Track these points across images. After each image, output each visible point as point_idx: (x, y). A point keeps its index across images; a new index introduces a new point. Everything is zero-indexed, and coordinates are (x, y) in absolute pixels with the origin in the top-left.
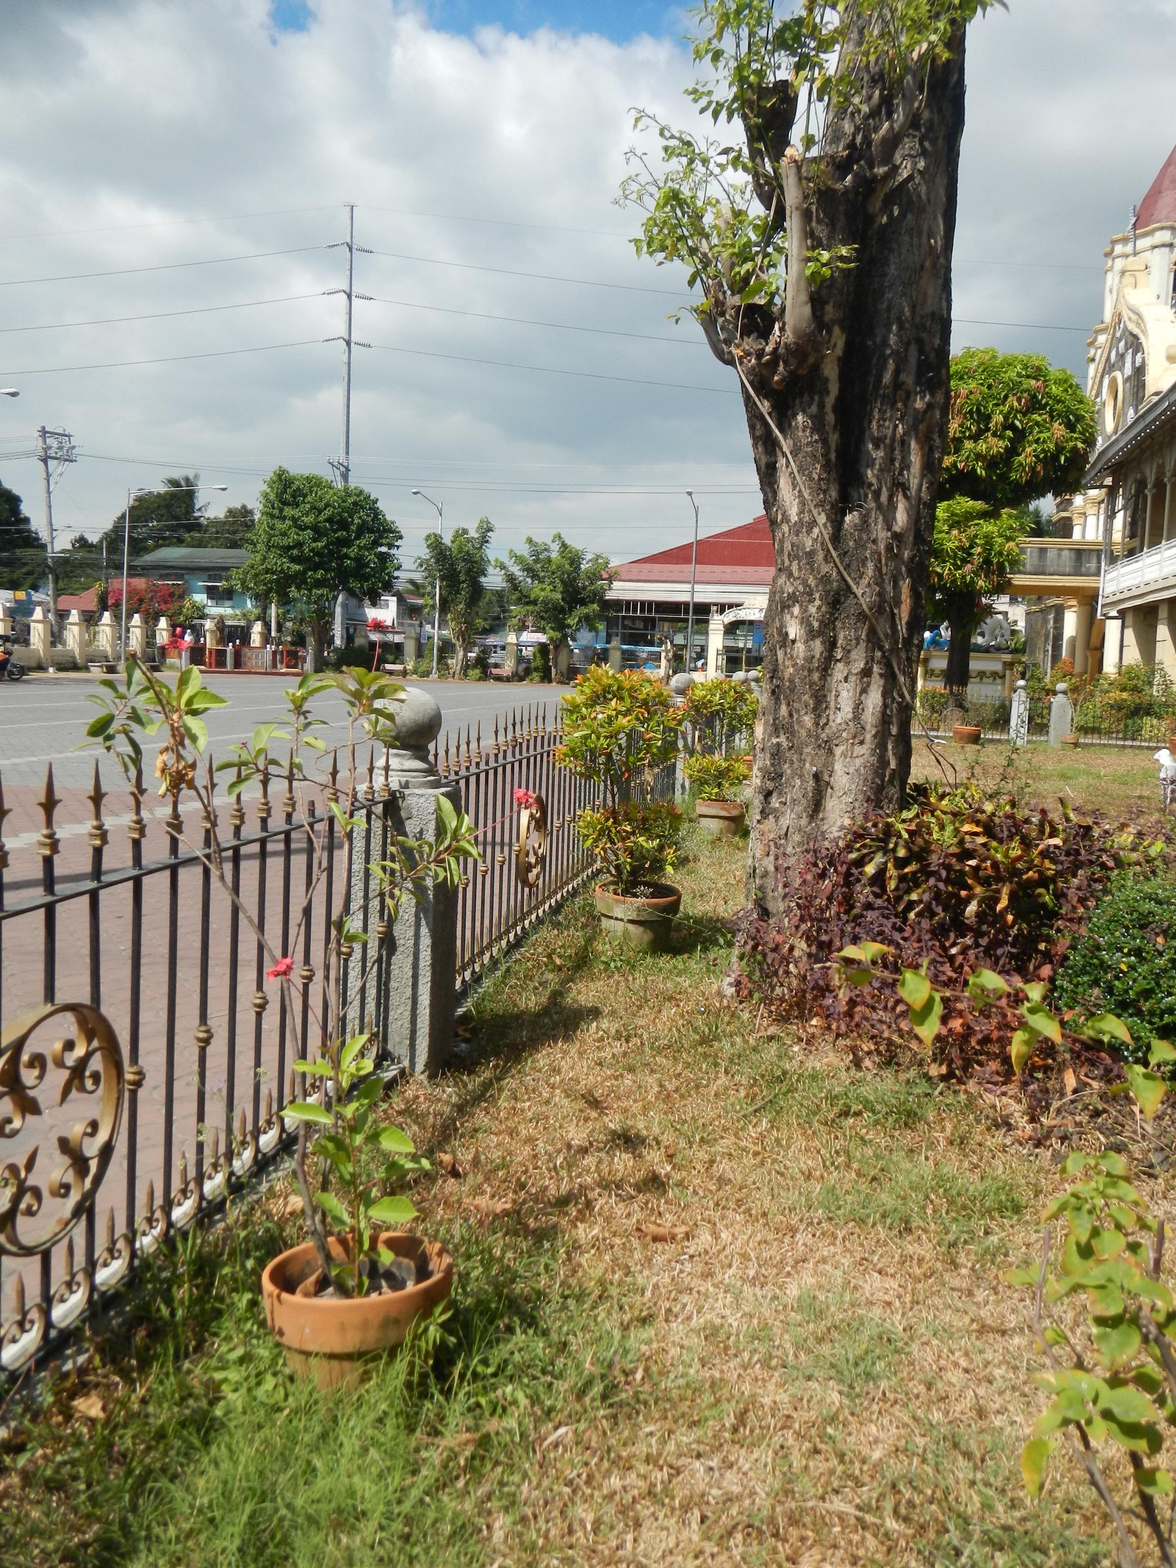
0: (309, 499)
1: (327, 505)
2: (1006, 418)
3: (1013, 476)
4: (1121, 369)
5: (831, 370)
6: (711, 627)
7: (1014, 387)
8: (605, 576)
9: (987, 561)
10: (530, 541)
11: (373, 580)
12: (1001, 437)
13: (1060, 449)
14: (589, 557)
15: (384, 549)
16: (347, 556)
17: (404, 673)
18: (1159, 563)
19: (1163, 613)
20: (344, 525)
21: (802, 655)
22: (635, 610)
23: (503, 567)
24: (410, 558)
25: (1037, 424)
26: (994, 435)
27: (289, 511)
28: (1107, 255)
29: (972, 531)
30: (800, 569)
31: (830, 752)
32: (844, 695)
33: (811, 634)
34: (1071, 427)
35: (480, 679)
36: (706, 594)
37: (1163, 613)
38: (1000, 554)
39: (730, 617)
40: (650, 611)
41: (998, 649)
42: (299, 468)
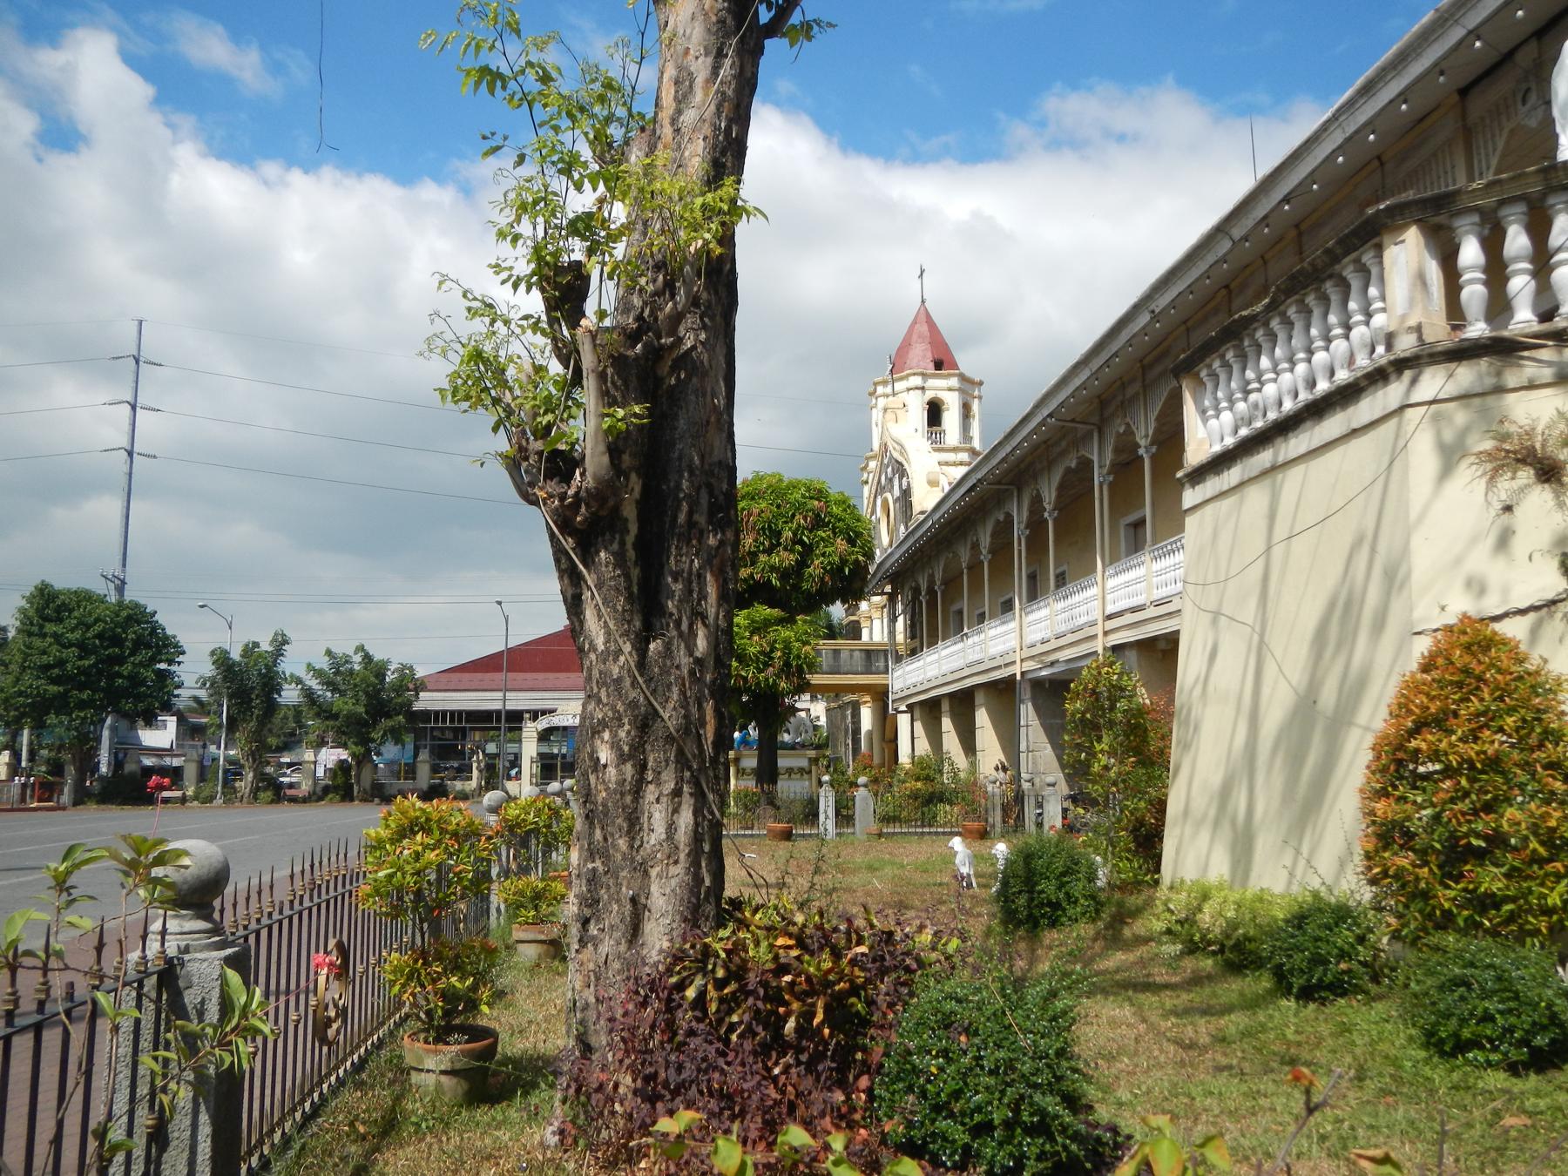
0: (76, 614)
1: (97, 620)
2: (795, 534)
3: (805, 586)
4: (891, 491)
5: (630, 512)
7: (799, 507)
8: (411, 686)
9: (787, 664)
10: (329, 653)
11: (151, 699)
12: (792, 551)
13: (844, 562)
15: (163, 666)
16: (119, 675)
17: (183, 800)
18: (937, 661)
19: (945, 706)
20: (117, 641)
21: (613, 779)
22: (444, 721)
23: (299, 681)
24: (193, 673)
25: (822, 539)
26: (785, 549)
27: (50, 628)
28: (871, 394)
29: (771, 636)
30: (608, 696)
31: (646, 874)
32: (657, 817)
33: (622, 758)
34: (851, 542)
35: (272, 802)
36: (518, 701)
37: (945, 706)
38: (799, 657)
39: (543, 723)
40: (460, 721)
41: (803, 746)
42: (63, 581)
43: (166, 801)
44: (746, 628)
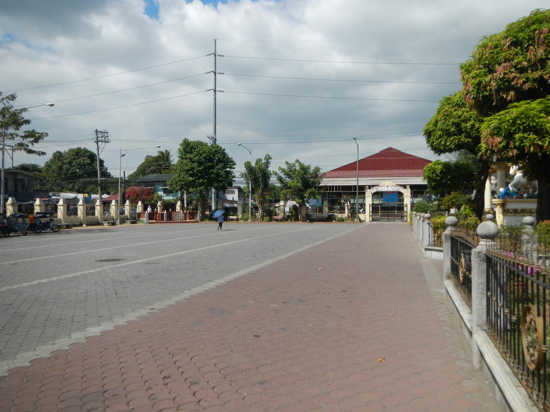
0: (196, 150)
1: (204, 152)
6: (366, 195)
10: (287, 163)
11: (225, 183)
14: (312, 168)
15: (228, 169)
16: (213, 173)
17: (238, 220)
20: (211, 160)
23: (276, 174)
24: (238, 170)
27: (188, 156)
35: (269, 221)
40: (339, 190)
42: (192, 138)
43: (232, 220)
44: (541, 112)
